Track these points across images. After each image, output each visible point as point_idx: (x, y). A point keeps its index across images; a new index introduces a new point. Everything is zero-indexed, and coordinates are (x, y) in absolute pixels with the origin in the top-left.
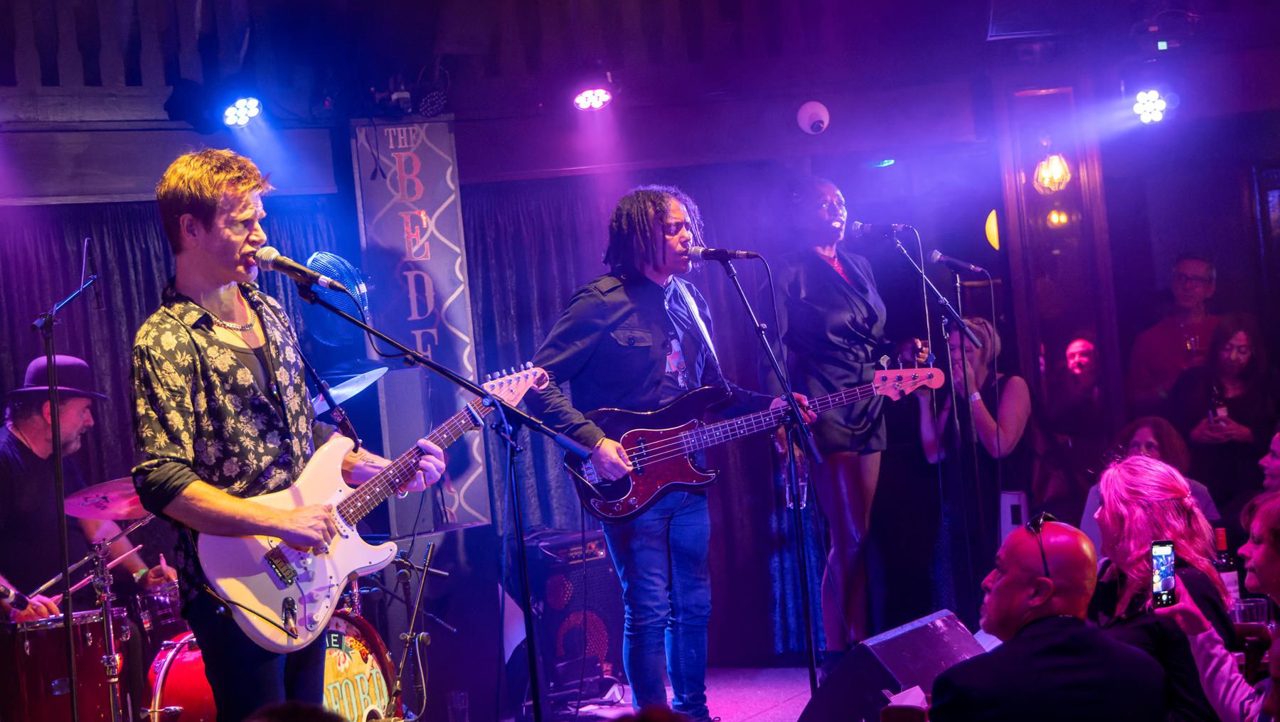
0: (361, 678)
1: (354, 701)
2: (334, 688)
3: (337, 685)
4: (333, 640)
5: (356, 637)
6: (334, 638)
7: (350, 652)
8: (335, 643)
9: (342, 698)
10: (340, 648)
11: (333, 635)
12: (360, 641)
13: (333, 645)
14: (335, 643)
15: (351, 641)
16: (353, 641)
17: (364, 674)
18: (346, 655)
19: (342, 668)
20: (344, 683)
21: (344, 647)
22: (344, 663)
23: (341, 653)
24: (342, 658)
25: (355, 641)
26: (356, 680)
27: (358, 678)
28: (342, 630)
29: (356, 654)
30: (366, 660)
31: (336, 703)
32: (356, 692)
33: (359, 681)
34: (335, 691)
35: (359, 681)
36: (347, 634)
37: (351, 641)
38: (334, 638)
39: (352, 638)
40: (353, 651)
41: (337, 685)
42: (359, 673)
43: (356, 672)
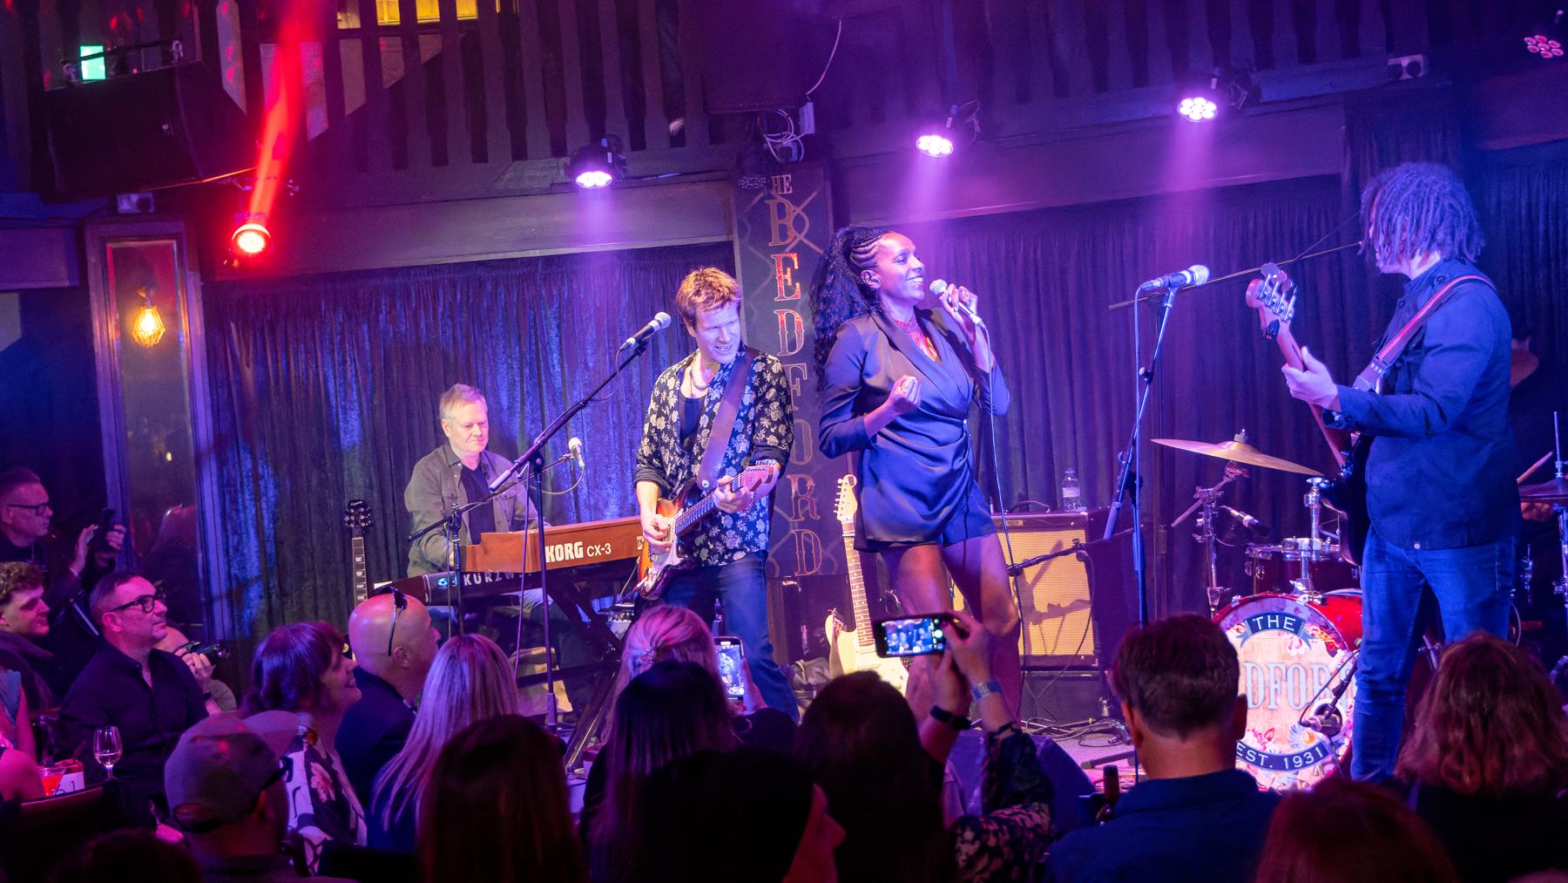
0: (1320, 669)
1: (1303, 687)
2: (1280, 668)
3: (1283, 667)
4: (1286, 623)
5: (1321, 627)
6: (1288, 621)
7: (1310, 640)
8: (1288, 626)
9: (1286, 680)
10: (1296, 632)
11: (1287, 618)
13: (1285, 627)
14: (1288, 626)
15: (1314, 630)
17: (1327, 666)
19: (1294, 652)
20: (1295, 666)
22: (1298, 648)
23: (1296, 638)
24: (1296, 642)
25: (1320, 630)
26: (1312, 670)
27: (1316, 668)
28: (1300, 616)
29: (1319, 644)
30: (1332, 651)
31: (1276, 683)
32: (1310, 679)
33: (1316, 671)
34: (1278, 672)
35: (1316, 671)
36: (1311, 621)
37: (1314, 630)
38: (1288, 621)
39: (1315, 627)
40: (1314, 640)
41: (1283, 667)
42: (1317, 664)
43: (1314, 660)
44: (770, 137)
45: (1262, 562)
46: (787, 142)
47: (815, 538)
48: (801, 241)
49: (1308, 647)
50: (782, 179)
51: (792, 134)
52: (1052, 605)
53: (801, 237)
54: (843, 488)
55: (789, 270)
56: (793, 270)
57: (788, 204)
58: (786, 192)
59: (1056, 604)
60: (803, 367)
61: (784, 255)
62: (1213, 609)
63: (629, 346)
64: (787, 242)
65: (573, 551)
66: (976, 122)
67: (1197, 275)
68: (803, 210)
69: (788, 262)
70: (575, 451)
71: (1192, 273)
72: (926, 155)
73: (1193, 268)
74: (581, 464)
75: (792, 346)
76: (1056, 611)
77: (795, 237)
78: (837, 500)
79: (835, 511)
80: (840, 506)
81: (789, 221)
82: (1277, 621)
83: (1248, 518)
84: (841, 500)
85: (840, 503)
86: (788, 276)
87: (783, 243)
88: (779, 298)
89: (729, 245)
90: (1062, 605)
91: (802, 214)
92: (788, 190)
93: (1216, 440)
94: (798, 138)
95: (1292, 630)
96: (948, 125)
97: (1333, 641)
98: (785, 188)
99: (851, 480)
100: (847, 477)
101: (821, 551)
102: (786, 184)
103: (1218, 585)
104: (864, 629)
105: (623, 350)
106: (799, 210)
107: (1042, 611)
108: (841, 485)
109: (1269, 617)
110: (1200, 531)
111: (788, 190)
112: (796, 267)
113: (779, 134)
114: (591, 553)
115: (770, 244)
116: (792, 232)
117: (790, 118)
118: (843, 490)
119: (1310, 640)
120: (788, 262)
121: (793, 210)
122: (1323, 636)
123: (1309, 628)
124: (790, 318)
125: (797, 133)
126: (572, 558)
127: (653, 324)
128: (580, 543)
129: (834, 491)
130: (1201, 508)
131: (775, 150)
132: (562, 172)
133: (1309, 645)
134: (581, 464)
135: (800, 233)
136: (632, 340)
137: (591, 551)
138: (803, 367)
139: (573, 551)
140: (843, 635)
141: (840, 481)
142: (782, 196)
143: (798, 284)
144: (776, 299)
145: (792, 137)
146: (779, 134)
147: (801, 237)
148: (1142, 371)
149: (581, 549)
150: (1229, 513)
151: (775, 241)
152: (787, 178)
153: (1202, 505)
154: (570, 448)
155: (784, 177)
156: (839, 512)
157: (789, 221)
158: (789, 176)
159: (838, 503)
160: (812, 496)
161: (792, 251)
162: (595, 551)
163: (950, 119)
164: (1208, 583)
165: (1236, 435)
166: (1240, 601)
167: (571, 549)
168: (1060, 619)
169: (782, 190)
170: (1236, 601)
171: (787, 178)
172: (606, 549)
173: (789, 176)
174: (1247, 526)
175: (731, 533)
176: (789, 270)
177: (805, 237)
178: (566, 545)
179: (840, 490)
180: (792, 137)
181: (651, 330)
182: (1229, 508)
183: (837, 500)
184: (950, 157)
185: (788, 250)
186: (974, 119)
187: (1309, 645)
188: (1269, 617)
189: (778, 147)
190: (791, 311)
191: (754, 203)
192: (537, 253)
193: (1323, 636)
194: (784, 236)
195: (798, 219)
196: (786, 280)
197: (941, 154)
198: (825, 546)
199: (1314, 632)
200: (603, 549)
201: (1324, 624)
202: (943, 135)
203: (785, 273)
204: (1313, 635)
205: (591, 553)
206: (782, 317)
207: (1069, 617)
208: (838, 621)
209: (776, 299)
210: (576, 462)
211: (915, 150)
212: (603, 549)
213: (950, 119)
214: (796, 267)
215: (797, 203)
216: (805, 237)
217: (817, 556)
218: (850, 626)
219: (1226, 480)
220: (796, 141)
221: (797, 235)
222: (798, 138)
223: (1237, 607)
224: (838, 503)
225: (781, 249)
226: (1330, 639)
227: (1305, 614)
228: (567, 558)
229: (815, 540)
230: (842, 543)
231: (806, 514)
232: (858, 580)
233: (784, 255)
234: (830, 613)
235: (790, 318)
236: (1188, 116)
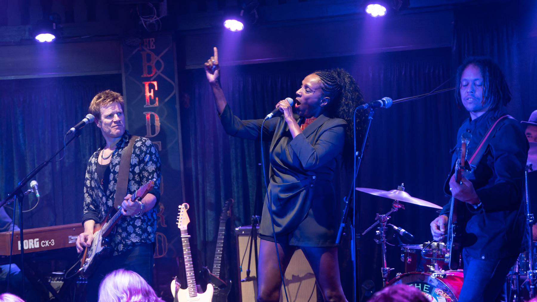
4: (425, 288)
6: (426, 287)
7: (438, 297)
8: (426, 289)
12: (448, 294)
13: (424, 290)
14: (426, 289)
16: (442, 292)
18: (434, 298)
21: (433, 293)
25: (443, 292)
28: (433, 284)
36: (437, 287)
38: (426, 287)
39: (440, 290)
40: (440, 297)
44: (143, 18)
45: (410, 254)
46: (152, 21)
47: (163, 237)
48: (159, 76)
49: (436, 301)
50: (149, 41)
51: (155, 16)
52: (295, 276)
53: (159, 72)
54: (181, 210)
55: (152, 90)
56: (155, 92)
57: (152, 54)
58: (151, 48)
59: (296, 275)
60: (159, 143)
61: (149, 82)
62: (384, 280)
63: (72, 131)
64: (152, 75)
65: (34, 243)
66: (256, 13)
67: (386, 102)
68: (161, 58)
69: (152, 87)
70: (34, 188)
71: (384, 101)
72: (229, 31)
73: (384, 99)
74: (38, 195)
75: (153, 132)
76: (296, 279)
77: (156, 73)
78: (178, 217)
79: (177, 223)
80: (180, 220)
81: (153, 63)
82: (420, 287)
83: (403, 230)
84: (180, 217)
85: (180, 218)
86: (152, 94)
87: (149, 76)
88: (147, 106)
89: (119, 76)
90: (301, 276)
91: (161, 61)
92: (153, 46)
93: (389, 189)
94: (158, 19)
95: (428, 291)
96: (242, 14)
97: (450, 298)
98: (151, 45)
99: (186, 206)
100: (184, 204)
101: (167, 244)
102: (152, 43)
103: (387, 267)
104: (192, 288)
105: (67, 135)
106: (158, 58)
107: (289, 279)
108: (180, 209)
109: (416, 284)
110: (379, 237)
111: (153, 46)
112: (156, 89)
113: (148, 16)
114: (43, 245)
115: (142, 76)
116: (154, 70)
117: (154, 8)
118: (181, 212)
119: (438, 297)
120: (152, 87)
121: (155, 58)
122: (445, 295)
123: (437, 291)
124: (152, 117)
125: (158, 16)
126: (33, 247)
127: (85, 120)
128: (38, 239)
129: (176, 212)
130: (379, 225)
131: (146, 25)
132: (27, 33)
133: (437, 300)
134: (38, 195)
135: (159, 69)
136: (73, 129)
137: (43, 244)
138: (158, 143)
139: (34, 243)
140: (180, 290)
141: (180, 207)
142: (150, 50)
143: (157, 99)
144: (145, 106)
145: (155, 18)
146: (148, 16)
147: (159, 72)
148: (357, 153)
149: (38, 243)
150: (393, 227)
151: (145, 75)
152: (152, 40)
153: (379, 223)
154: (31, 186)
155: (151, 39)
156: (179, 224)
157: (153, 63)
158: (153, 39)
159: (179, 218)
160: (163, 214)
161: (154, 81)
162: (45, 243)
163: (242, 11)
164: (381, 265)
165: (399, 186)
166: (400, 276)
167: (32, 242)
168: (299, 283)
169: (150, 47)
170: (398, 276)
171: (152, 40)
172: (52, 243)
173: (153, 39)
174: (401, 234)
175: (133, 235)
176: (152, 90)
177: (162, 72)
178: (30, 240)
179: (179, 212)
180: (155, 18)
181: (84, 123)
182: (392, 225)
183: (178, 217)
184: (242, 31)
185: (152, 79)
186: (255, 11)
187: (437, 300)
188: (416, 284)
189: (147, 23)
190: (153, 113)
191: (134, 53)
192: (13, 78)
193: (445, 295)
194: (150, 72)
195: (158, 63)
196: (150, 96)
197: (237, 30)
198: (169, 242)
199: (440, 293)
200: (50, 243)
201: (445, 289)
202: (238, 20)
203: (150, 92)
204: (439, 294)
205: (43, 245)
206: (148, 116)
207: (303, 282)
208: (178, 283)
209: (145, 106)
210: (35, 194)
211: (224, 28)
212: (50, 243)
213: (242, 11)
214: (156, 89)
215: (157, 54)
216: (162, 72)
217: (165, 247)
218: (184, 286)
219: (393, 210)
220: (157, 20)
221: (157, 71)
222: (158, 19)
223: (399, 279)
224: (179, 218)
225: (148, 79)
226: (448, 297)
227: (435, 283)
228: (30, 248)
229: (164, 239)
230: (181, 242)
231: (159, 224)
232: (189, 261)
233: (149, 82)
234: (174, 279)
235: (152, 117)
236: (371, 14)
